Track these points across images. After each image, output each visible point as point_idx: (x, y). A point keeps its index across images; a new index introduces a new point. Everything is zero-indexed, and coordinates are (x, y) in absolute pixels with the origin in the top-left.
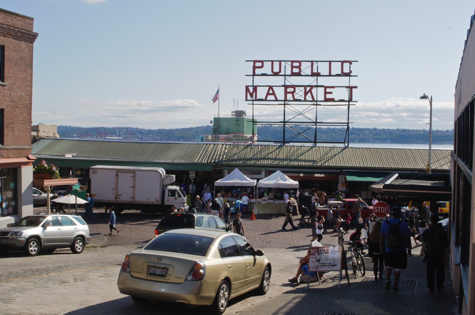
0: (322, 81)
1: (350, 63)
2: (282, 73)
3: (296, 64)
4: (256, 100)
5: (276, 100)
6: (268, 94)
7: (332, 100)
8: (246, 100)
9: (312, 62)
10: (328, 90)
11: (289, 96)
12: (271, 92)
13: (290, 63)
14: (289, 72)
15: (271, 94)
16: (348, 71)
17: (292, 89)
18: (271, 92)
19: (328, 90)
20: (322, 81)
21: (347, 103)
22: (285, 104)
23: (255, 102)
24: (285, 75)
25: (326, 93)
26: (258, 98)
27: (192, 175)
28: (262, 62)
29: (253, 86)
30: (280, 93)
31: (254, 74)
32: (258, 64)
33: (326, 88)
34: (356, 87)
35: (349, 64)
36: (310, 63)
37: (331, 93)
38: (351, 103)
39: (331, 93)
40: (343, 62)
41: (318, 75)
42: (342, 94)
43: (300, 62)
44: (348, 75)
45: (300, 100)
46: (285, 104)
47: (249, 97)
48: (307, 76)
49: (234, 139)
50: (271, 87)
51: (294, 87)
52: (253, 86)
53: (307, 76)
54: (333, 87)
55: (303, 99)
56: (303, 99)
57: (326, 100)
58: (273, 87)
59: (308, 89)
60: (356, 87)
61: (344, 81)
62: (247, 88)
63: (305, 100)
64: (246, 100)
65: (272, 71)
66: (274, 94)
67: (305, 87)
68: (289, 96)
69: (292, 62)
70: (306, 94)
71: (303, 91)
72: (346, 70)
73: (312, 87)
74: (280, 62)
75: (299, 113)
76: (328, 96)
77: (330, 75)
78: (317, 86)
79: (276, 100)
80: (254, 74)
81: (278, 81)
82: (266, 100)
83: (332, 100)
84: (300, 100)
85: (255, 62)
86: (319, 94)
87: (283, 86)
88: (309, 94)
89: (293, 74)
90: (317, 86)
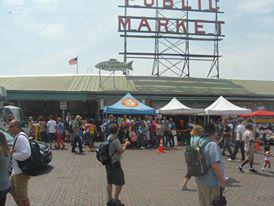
0: (192, 16)
2: (154, 6)
4: (130, 31)
6: (142, 25)
8: (120, 30)
10: (199, 24)
11: (162, 28)
14: (161, 5)
17: (165, 22)
19: (199, 24)
20: (192, 16)
23: (128, 34)
24: (157, 8)
25: (197, 26)
27: (63, 106)
30: (153, 24)
31: (127, 6)
33: (196, 21)
34: (223, 23)
37: (202, 27)
39: (202, 27)
41: (188, 9)
42: (210, 28)
44: (215, 11)
47: (122, 28)
48: (177, 9)
51: (167, 20)
53: (177, 9)
56: (175, 30)
57: (197, 33)
58: (148, 21)
60: (223, 23)
61: (211, 16)
62: (120, 18)
63: (177, 33)
64: (120, 30)
65: (145, 3)
66: (147, 25)
67: (178, 20)
68: (162, 28)
70: (178, 26)
72: (214, 6)
75: (170, 45)
76: (199, 29)
77: (200, 10)
78: (187, 20)
79: (150, 31)
80: (127, 6)
82: (139, 31)
83: (203, 33)
86: (191, 28)
88: (181, 27)
89: (165, 7)
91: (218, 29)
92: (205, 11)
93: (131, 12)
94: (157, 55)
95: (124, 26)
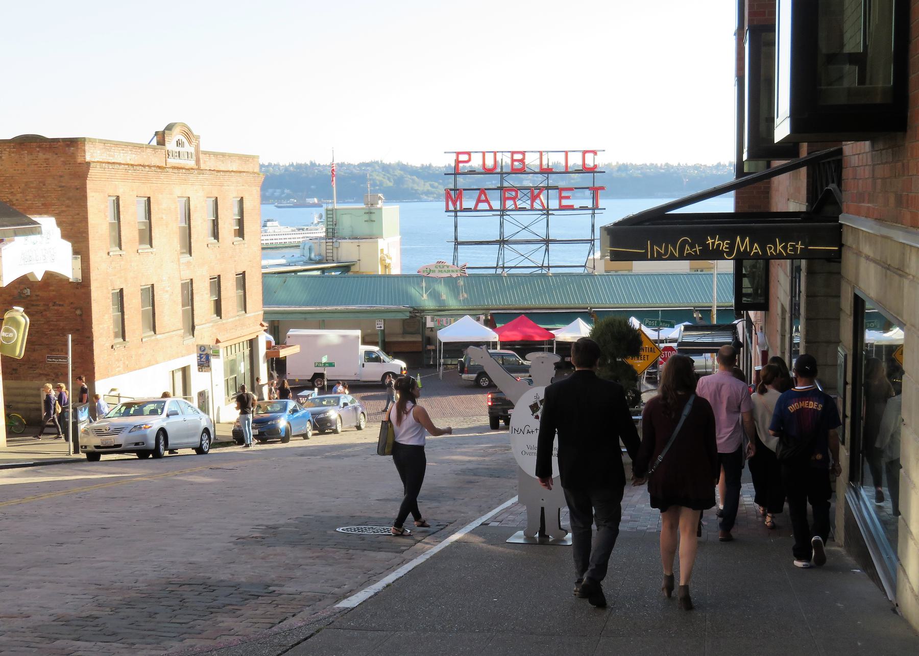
0: (553, 180)
1: (595, 152)
3: (518, 157)
4: (461, 211)
5: (491, 210)
6: (479, 201)
7: (571, 208)
8: (447, 211)
9: (541, 153)
12: (483, 197)
13: (509, 155)
15: (483, 201)
16: (592, 165)
17: (514, 193)
18: (483, 197)
19: (564, 194)
21: (591, 212)
22: (502, 216)
23: (459, 214)
26: (464, 207)
28: (469, 153)
29: (455, 190)
32: (463, 158)
33: (561, 190)
34: (602, 188)
35: (591, 155)
36: (538, 155)
38: (596, 211)
39: (568, 198)
40: (584, 152)
43: (523, 153)
45: (524, 209)
46: (502, 216)
47: (451, 207)
49: (437, 270)
50: (482, 191)
52: (455, 190)
54: (570, 189)
55: (528, 207)
56: (528, 207)
57: (562, 208)
59: (536, 192)
60: (602, 188)
63: (532, 209)
64: (447, 211)
66: (487, 201)
69: (513, 153)
71: (529, 195)
73: (541, 189)
74: (495, 153)
76: (565, 202)
78: (548, 188)
79: (491, 210)
81: (493, 182)
82: (476, 210)
83: (571, 208)
84: (524, 209)
85: (458, 153)
87: (498, 189)
88: (538, 201)
89: (515, 171)
90: (548, 188)
91: (595, 198)
92: (577, 172)
93: (462, 182)
94: (502, 242)
95: (454, 204)
